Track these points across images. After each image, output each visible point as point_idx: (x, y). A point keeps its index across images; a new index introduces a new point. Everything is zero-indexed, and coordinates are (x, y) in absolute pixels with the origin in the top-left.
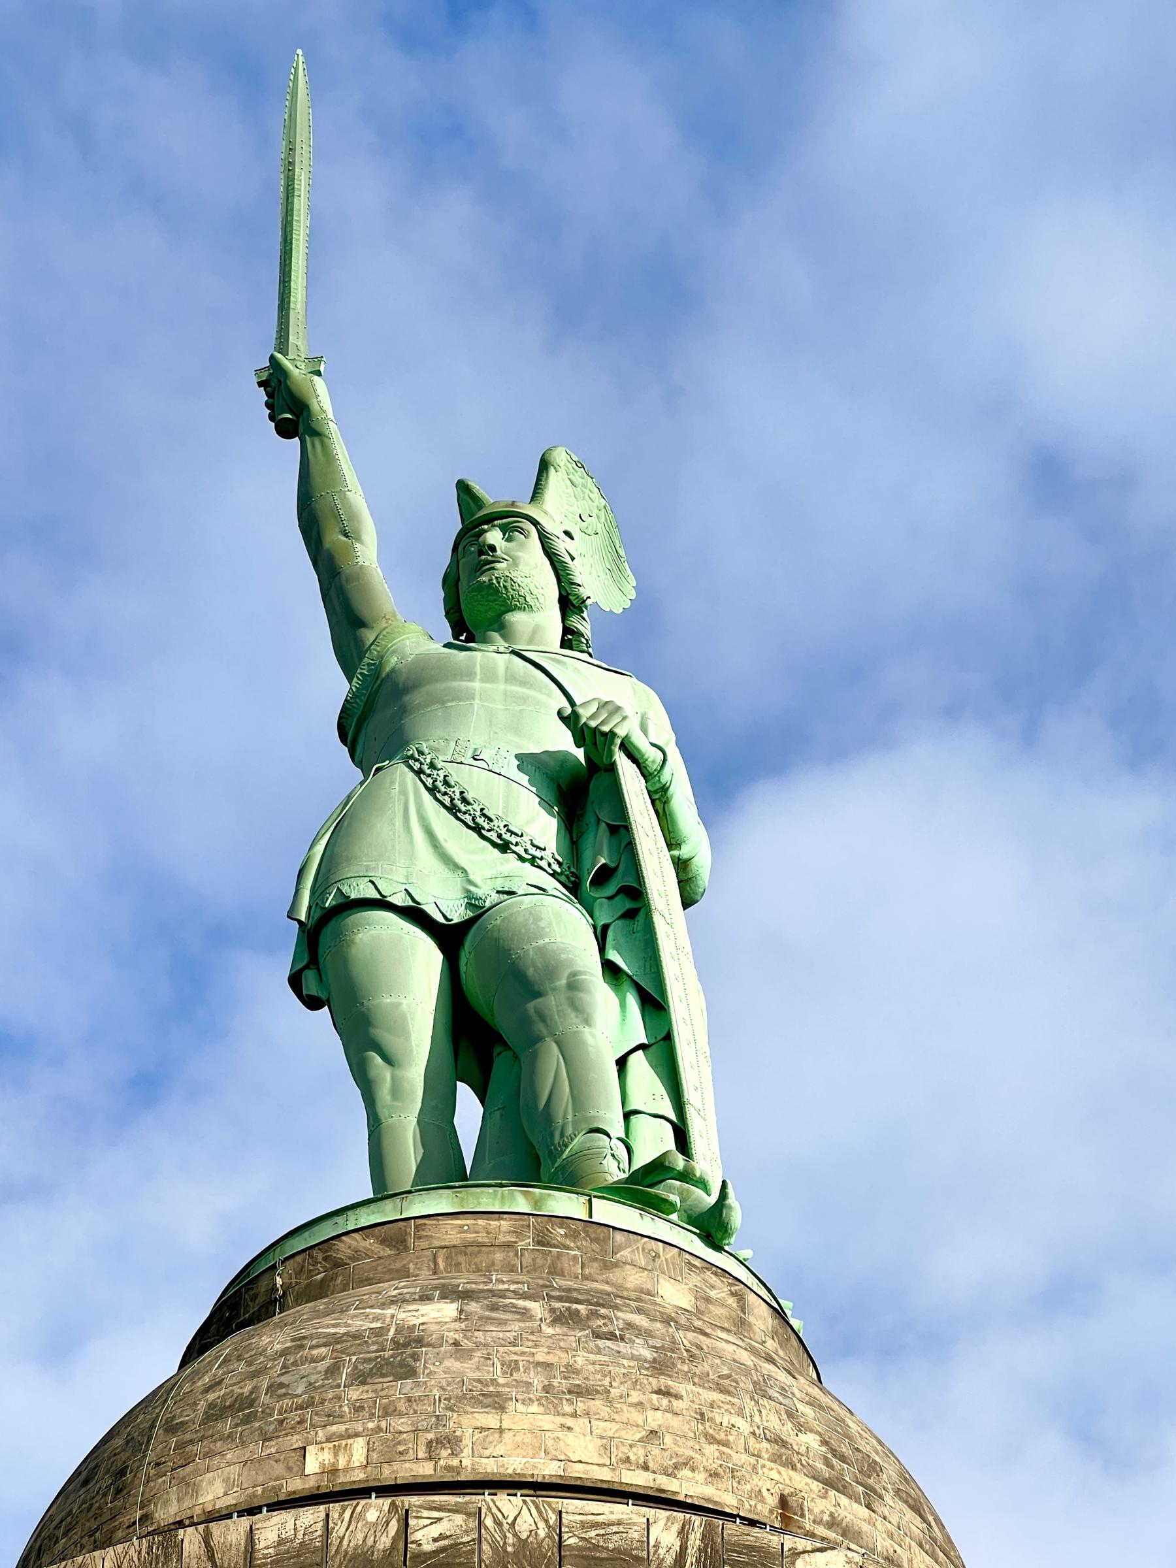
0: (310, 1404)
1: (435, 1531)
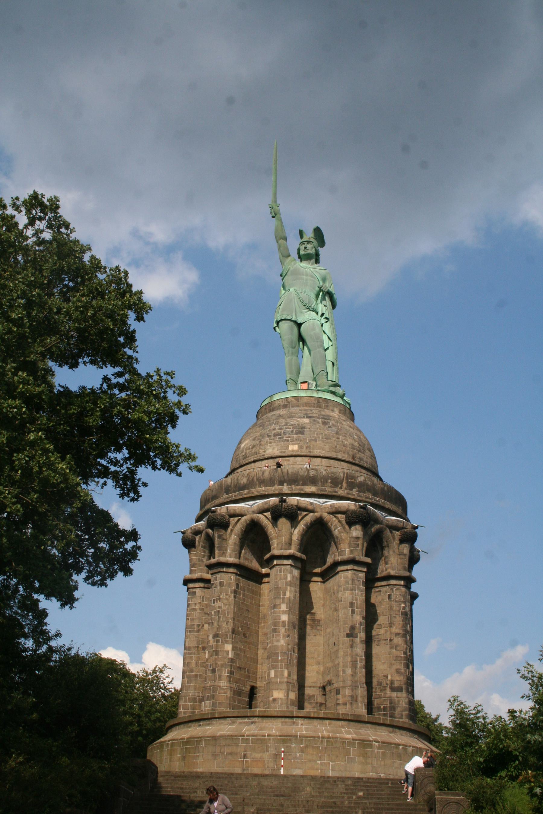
0: (289, 437)
1: (312, 473)
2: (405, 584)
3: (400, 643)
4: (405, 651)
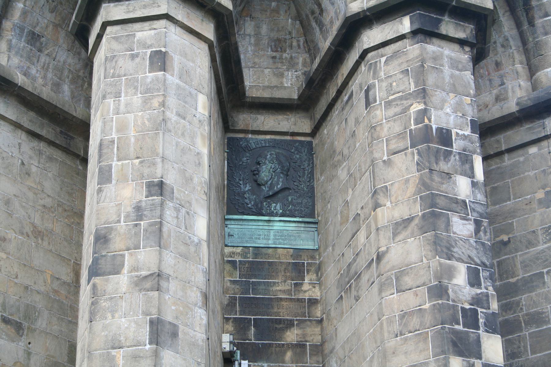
2: (416, 26)
3: (414, 257)
4: (434, 283)
